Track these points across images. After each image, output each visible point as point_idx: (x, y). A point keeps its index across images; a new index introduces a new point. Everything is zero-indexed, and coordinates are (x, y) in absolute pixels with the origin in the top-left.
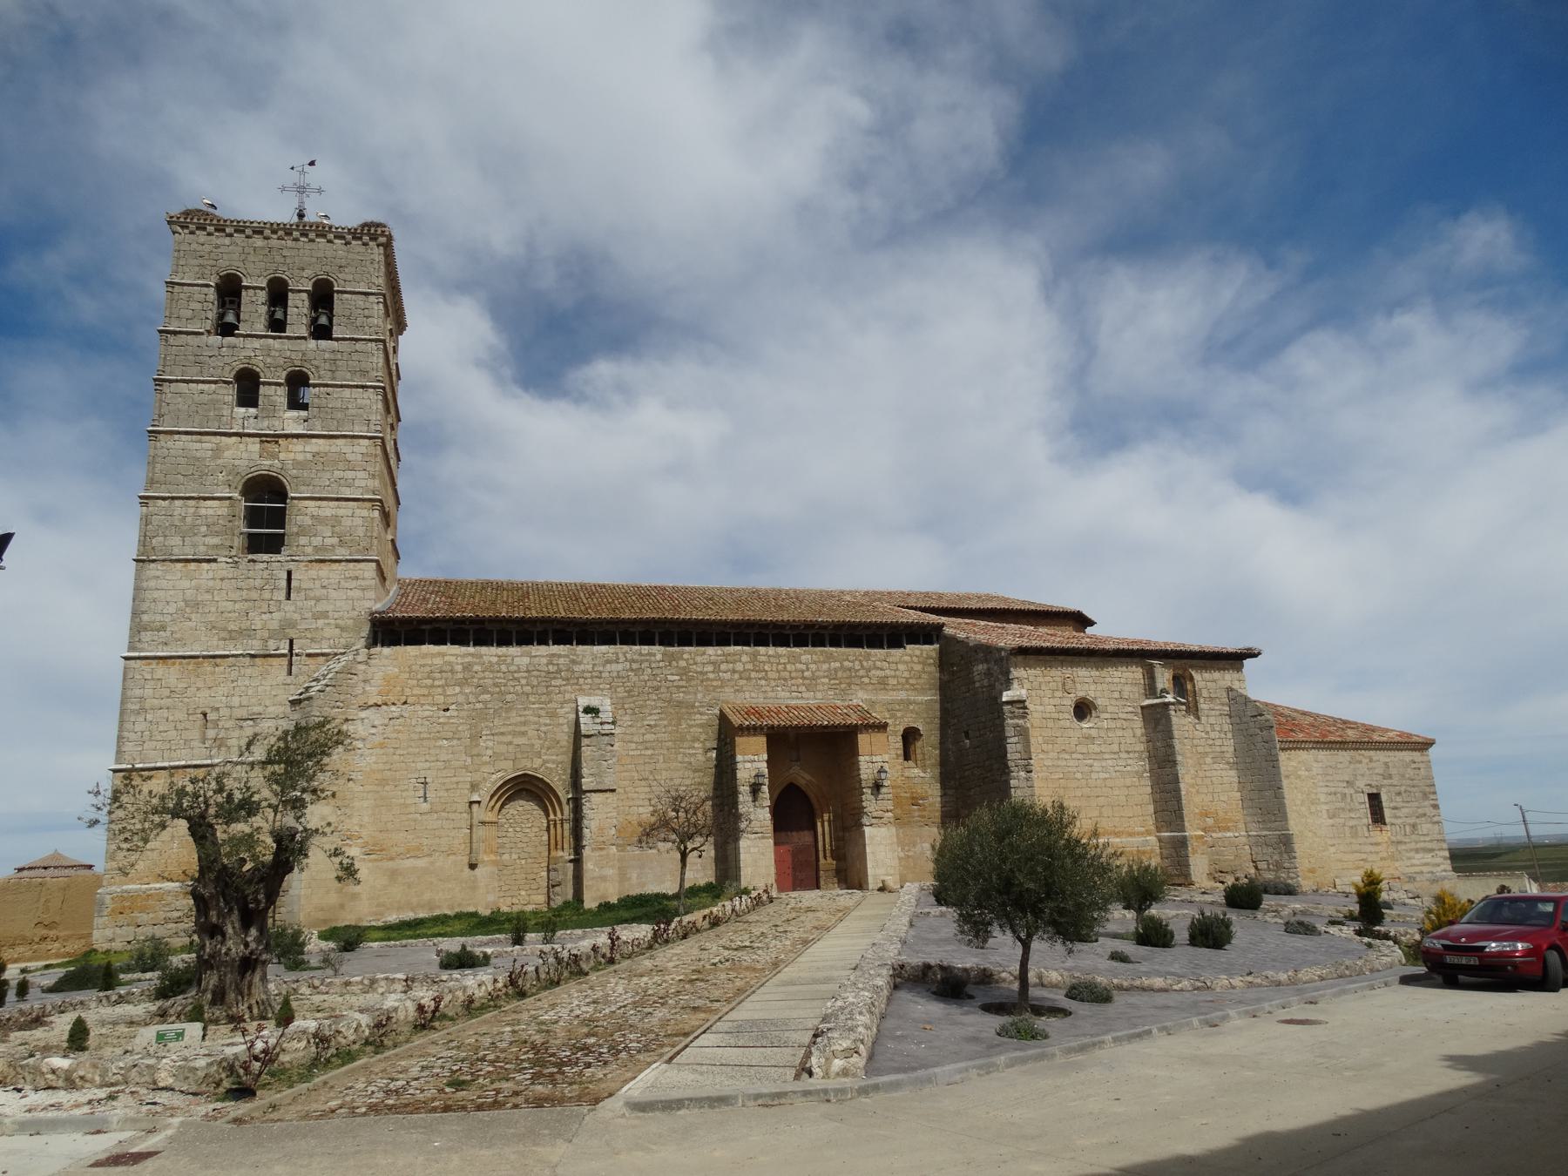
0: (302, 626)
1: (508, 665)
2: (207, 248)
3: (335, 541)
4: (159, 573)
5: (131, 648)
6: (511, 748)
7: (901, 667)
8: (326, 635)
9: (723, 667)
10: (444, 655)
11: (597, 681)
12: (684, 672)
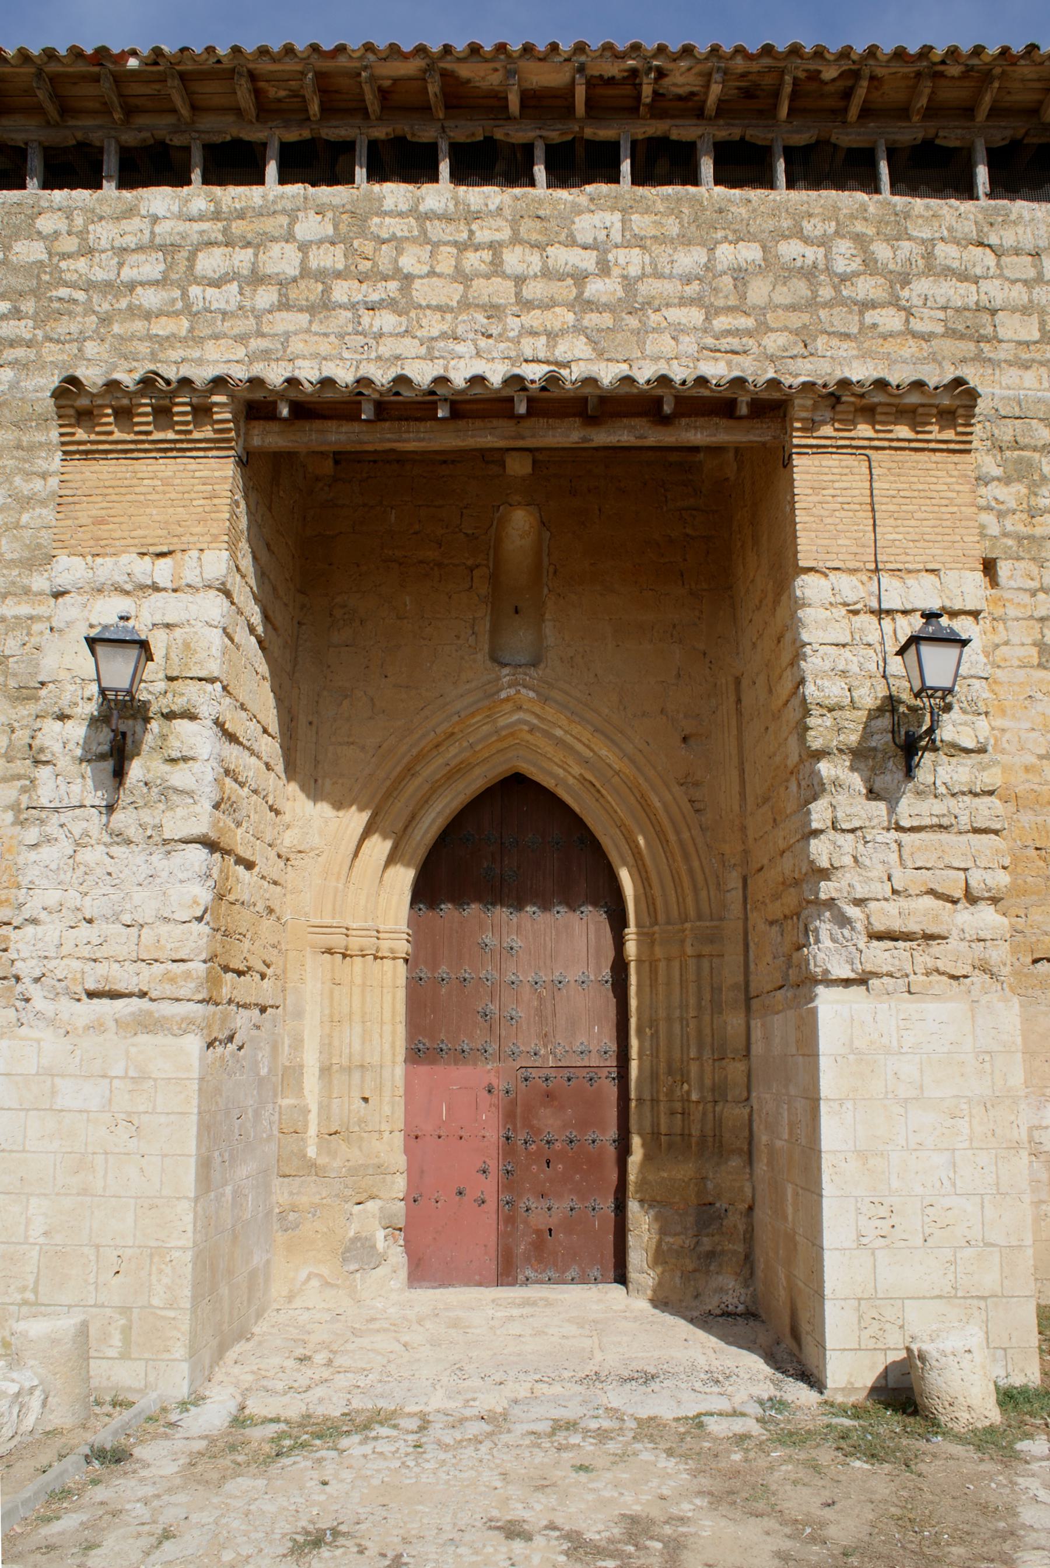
9: (210, 262)
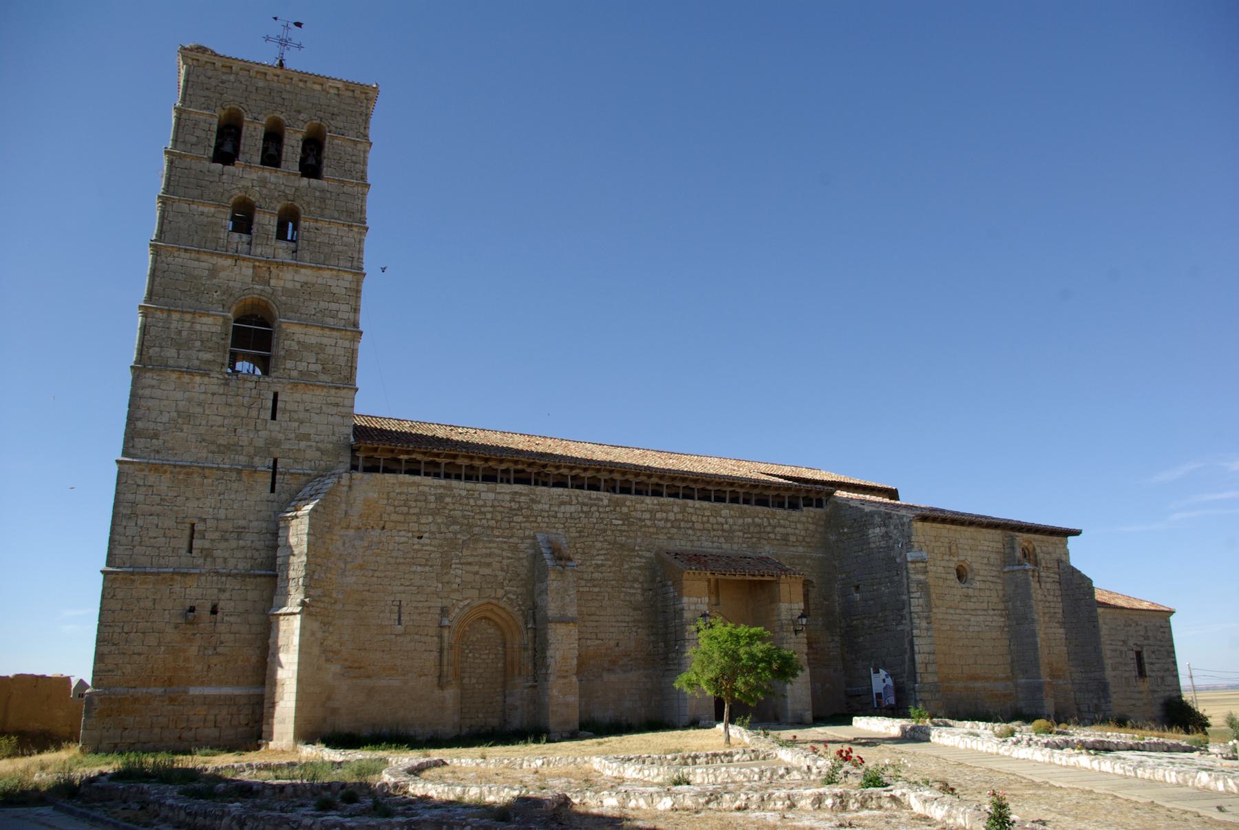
0: (286, 446)
1: (476, 499)
2: (213, 82)
3: (319, 367)
4: (154, 382)
5: (125, 453)
6: (477, 577)
7: (799, 526)
8: (308, 456)
9: (659, 515)
10: (419, 485)
11: (553, 520)
12: (626, 518)
